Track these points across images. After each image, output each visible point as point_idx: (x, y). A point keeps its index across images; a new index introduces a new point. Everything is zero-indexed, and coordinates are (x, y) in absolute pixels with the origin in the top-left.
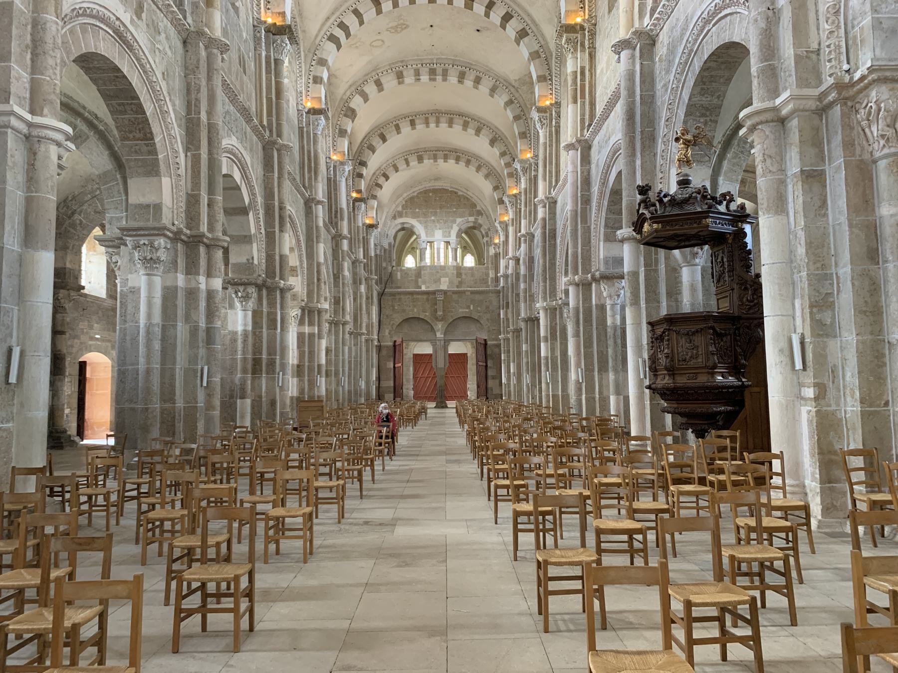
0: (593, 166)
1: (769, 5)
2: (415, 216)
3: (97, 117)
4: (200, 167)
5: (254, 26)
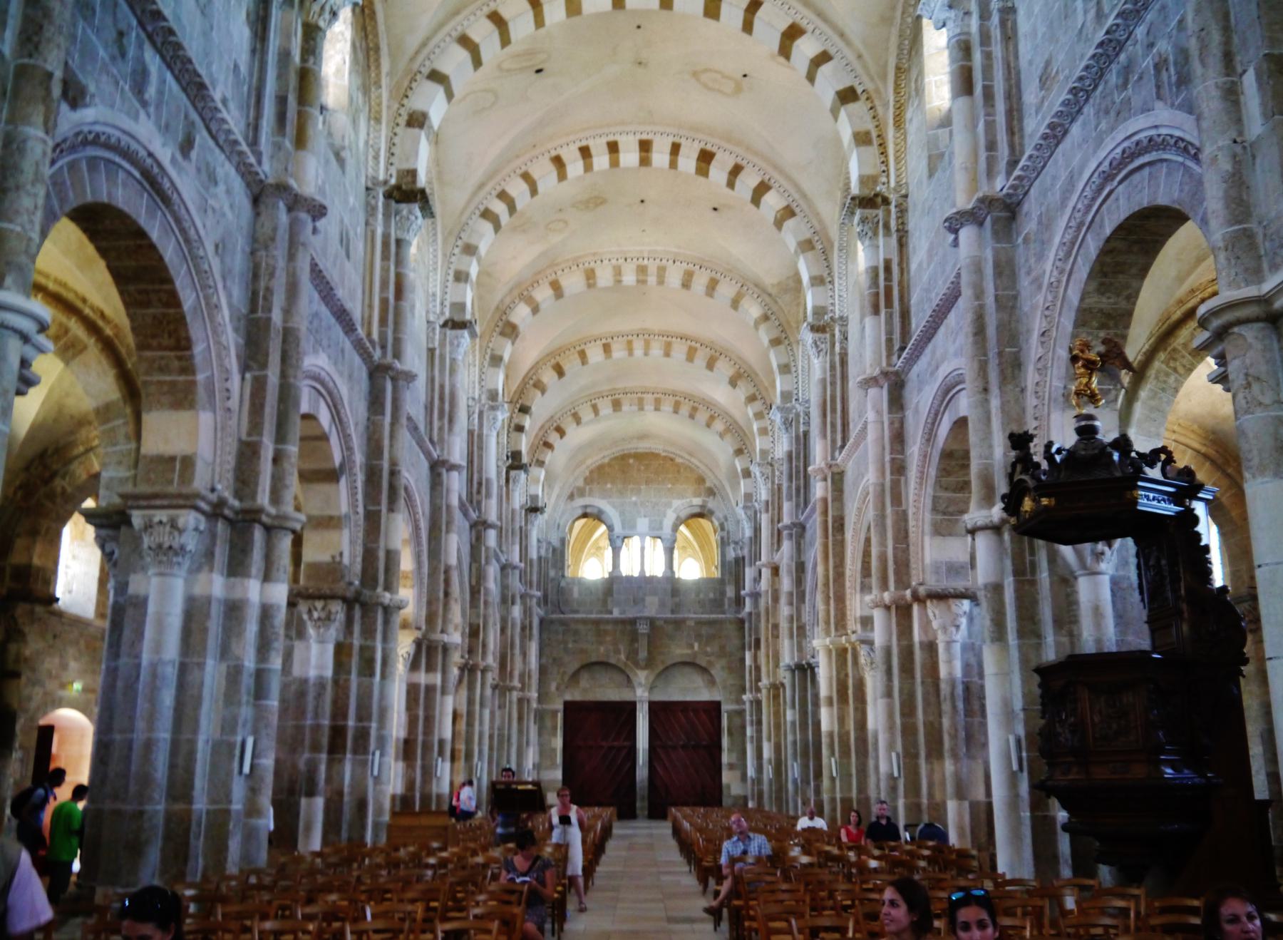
0: (909, 414)
1: (1234, 135)
2: (605, 495)
3: (103, 315)
4: (264, 398)
5: (367, 189)
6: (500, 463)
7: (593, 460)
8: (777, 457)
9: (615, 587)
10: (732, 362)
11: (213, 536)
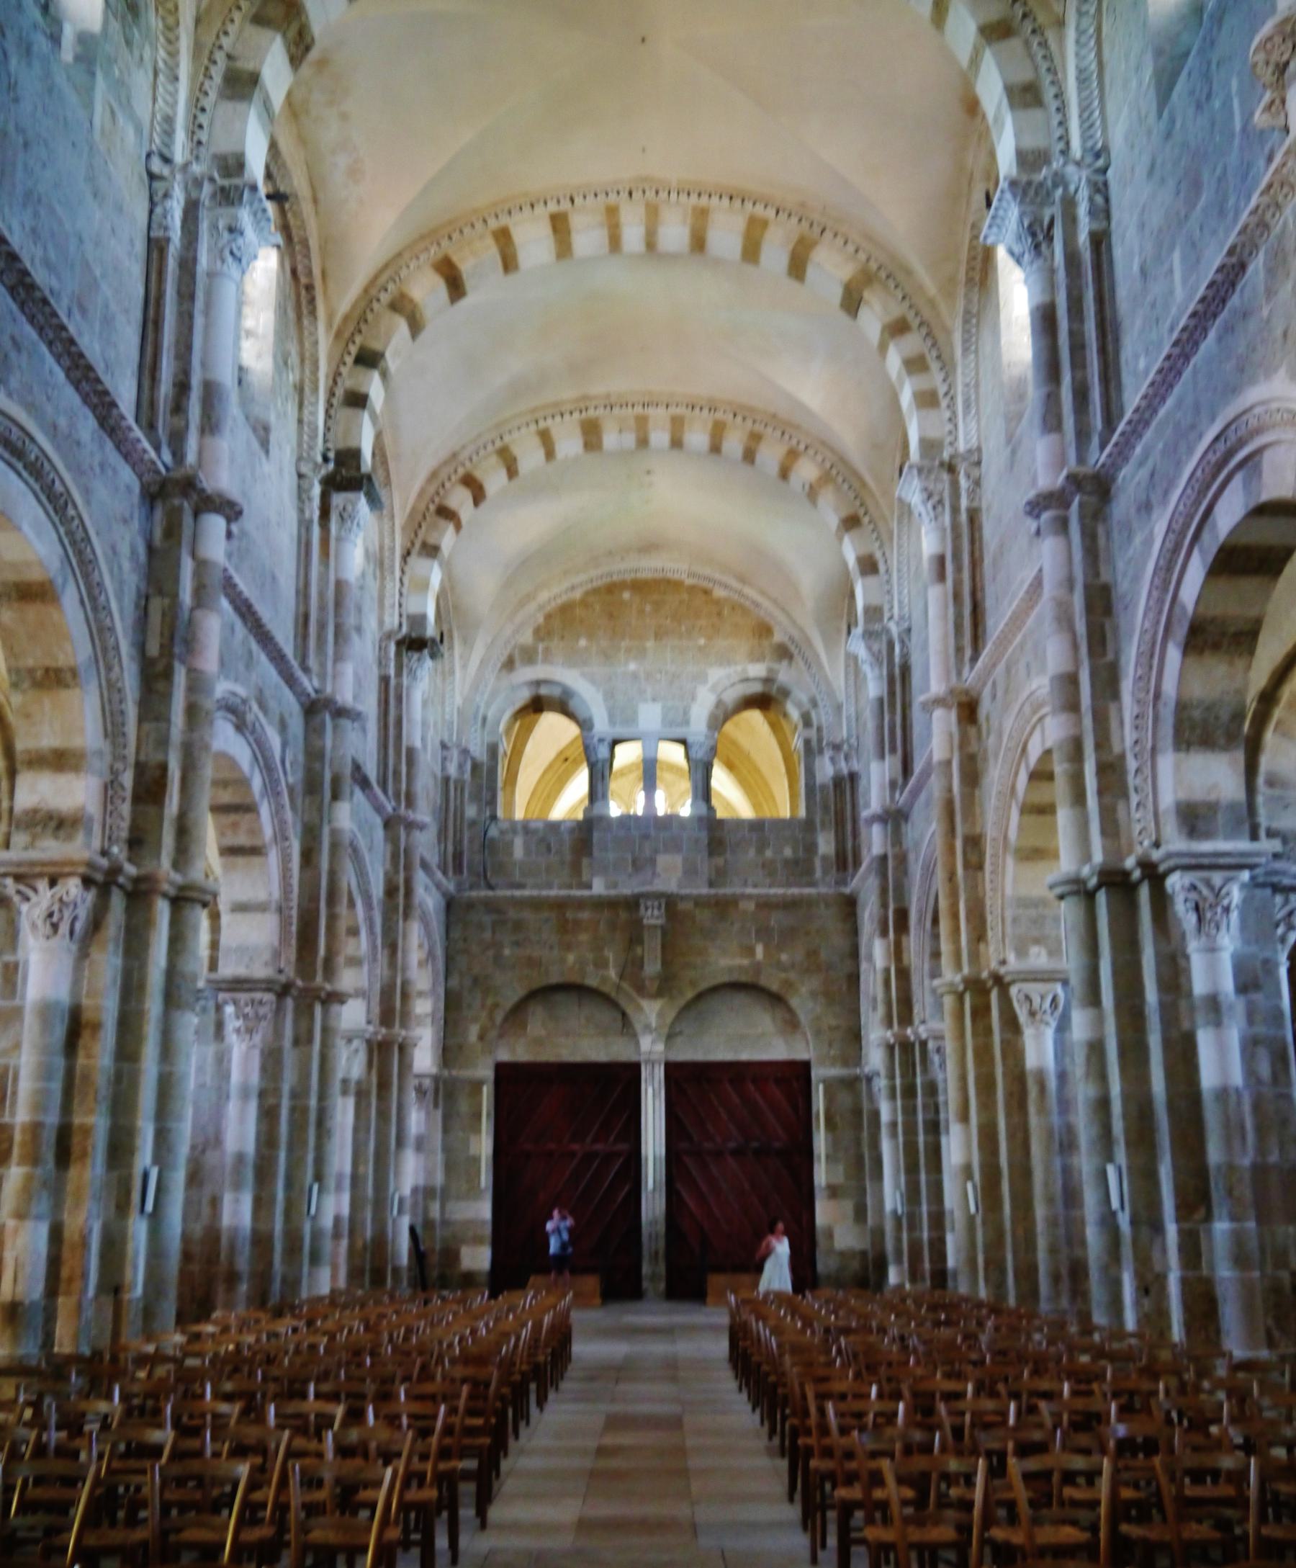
2: (574, 659)
6: (305, 469)
7: (553, 593)
8: (962, 447)
9: (596, 836)
10: (851, 248)
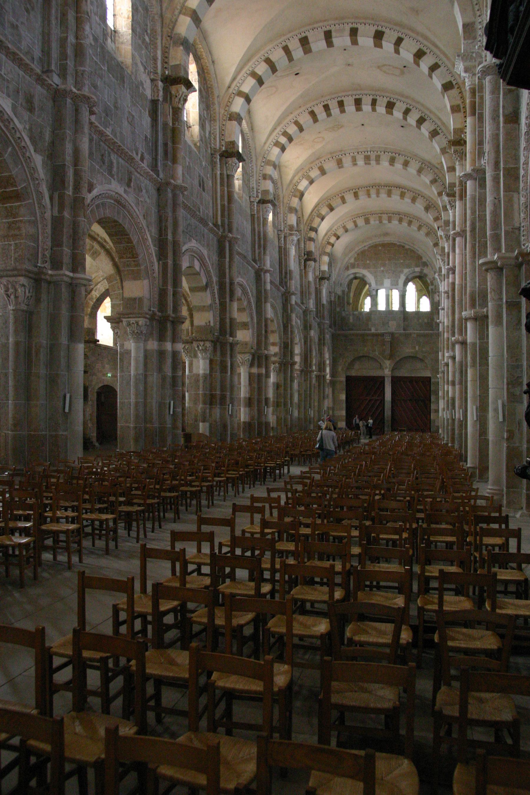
2: (366, 267)
11: (152, 327)
